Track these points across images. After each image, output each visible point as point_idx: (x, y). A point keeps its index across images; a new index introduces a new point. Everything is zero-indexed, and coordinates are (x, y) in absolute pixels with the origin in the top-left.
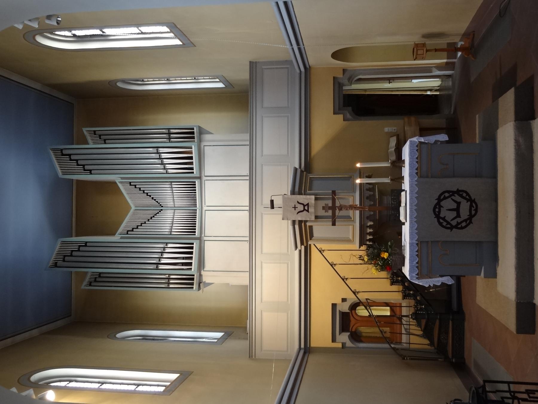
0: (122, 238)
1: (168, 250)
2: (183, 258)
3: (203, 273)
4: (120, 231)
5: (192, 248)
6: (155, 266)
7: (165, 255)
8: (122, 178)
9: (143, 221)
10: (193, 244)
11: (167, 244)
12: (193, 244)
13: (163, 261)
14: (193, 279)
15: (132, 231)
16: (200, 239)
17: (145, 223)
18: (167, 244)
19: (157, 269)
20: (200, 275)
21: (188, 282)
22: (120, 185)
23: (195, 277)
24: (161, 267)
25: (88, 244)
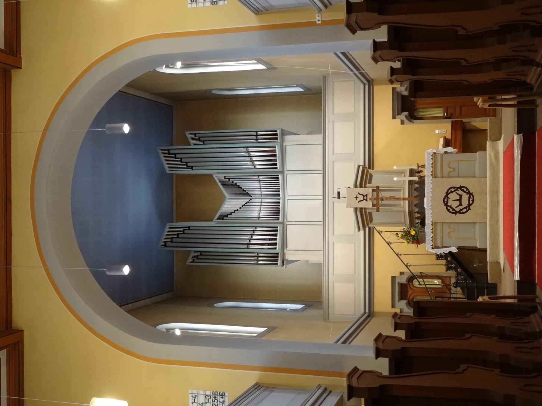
0: (218, 223)
2: (269, 239)
3: (285, 251)
4: (217, 217)
5: (276, 231)
6: (246, 246)
7: (255, 237)
8: (218, 173)
10: (277, 227)
11: (256, 227)
12: (277, 227)
14: (277, 257)
15: (227, 217)
16: (283, 223)
17: (237, 210)
18: (256, 227)
19: (248, 248)
20: (284, 254)
21: (274, 259)
22: (216, 179)
23: (279, 255)
24: (251, 247)
25: (191, 228)
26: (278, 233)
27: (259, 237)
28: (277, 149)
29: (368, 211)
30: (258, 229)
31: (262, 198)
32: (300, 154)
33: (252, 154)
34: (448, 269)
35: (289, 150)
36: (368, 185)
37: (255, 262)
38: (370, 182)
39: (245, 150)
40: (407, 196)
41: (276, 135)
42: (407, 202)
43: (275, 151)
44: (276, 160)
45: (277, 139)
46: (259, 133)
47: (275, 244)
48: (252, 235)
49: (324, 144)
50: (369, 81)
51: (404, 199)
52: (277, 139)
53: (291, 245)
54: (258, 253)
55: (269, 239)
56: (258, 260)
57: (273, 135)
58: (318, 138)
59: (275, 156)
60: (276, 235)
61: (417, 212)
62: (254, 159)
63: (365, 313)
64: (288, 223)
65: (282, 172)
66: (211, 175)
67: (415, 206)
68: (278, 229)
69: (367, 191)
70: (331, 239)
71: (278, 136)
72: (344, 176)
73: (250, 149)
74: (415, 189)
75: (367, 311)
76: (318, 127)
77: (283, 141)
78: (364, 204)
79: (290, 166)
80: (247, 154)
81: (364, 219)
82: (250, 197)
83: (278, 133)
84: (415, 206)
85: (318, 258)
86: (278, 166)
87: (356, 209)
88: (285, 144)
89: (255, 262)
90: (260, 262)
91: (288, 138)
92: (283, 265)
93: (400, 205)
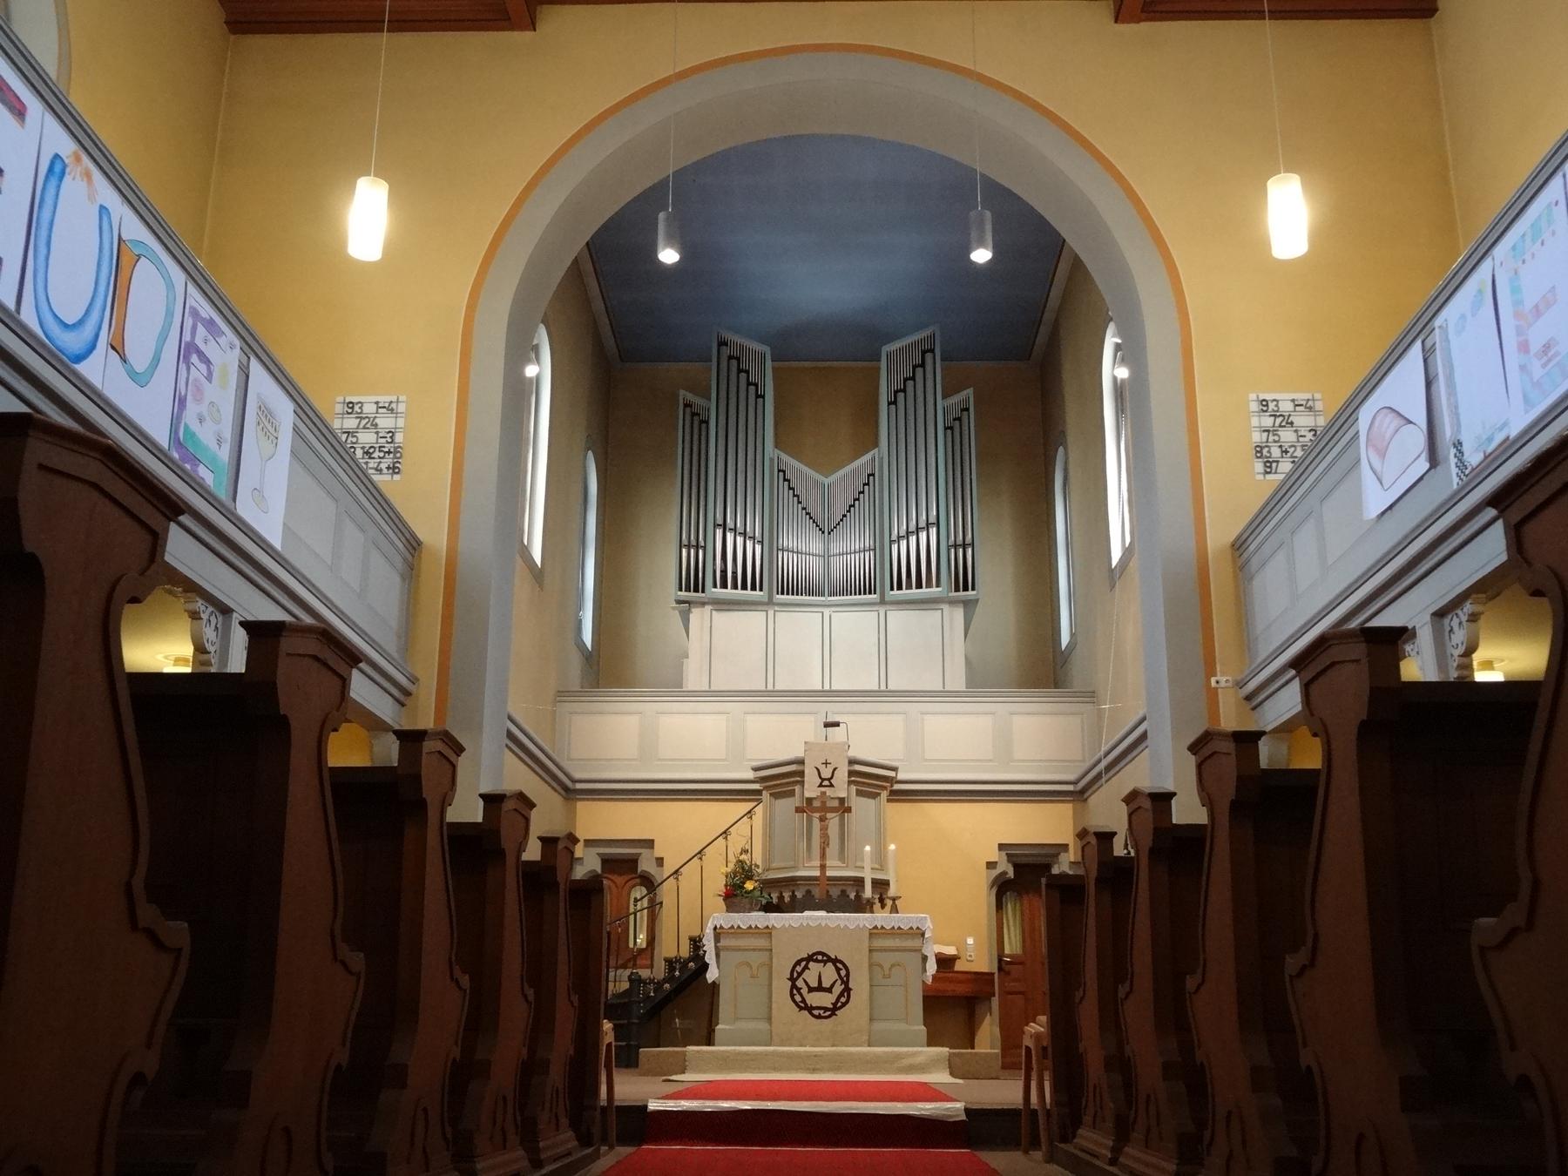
0: (772, 460)
1: (749, 544)
2: (735, 573)
3: (708, 608)
4: (784, 457)
5: (754, 588)
6: (720, 521)
7: (740, 540)
9: (802, 498)
11: (762, 543)
13: (730, 537)
14: (696, 590)
16: (770, 602)
19: (716, 526)
20: (703, 604)
21: (693, 582)
22: (868, 456)
24: (719, 532)
26: (749, 592)
27: (741, 550)
28: (934, 589)
29: (797, 788)
30: (758, 548)
31: (826, 556)
32: (923, 641)
33: (923, 536)
34: (670, 963)
35: (932, 617)
36: (854, 788)
37: (685, 541)
38: (860, 793)
39: (933, 519)
40: (829, 873)
41: (966, 589)
42: (817, 873)
43: (929, 585)
44: (909, 587)
45: (957, 590)
46: (969, 551)
47: (724, 586)
48: (744, 534)
49: (944, 694)
50: (1083, 792)
51: (823, 867)
52: (957, 590)
53: (723, 619)
54: (704, 548)
55: (735, 573)
56: (689, 547)
57: (964, 581)
58: (958, 681)
59: (919, 586)
60: (744, 587)
61: (793, 896)
62: (913, 539)
63: (575, 781)
64: (771, 613)
65: (883, 602)
66: (876, 444)
67: (809, 892)
68: (758, 592)
69: (841, 789)
70: (735, 708)
71: (962, 593)
72: (873, 737)
73: (933, 531)
74: (843, 892)
75: (579, 786)
76: (981, 680)
77: (952, 602)
78: (811, 779)
79: (897, 618)
80: (922, 524)
81: (779, 781)
82: (827, 530)
83: (970, 592)
84: (809, 892)
85: (694, 678)
86: (895, 592)
87: (801, 762)
88: (945, 607)
89: (685, 541)
90: (684, 551)
91: (958, 614)
92: (679, 602)
93: (810, 858)
